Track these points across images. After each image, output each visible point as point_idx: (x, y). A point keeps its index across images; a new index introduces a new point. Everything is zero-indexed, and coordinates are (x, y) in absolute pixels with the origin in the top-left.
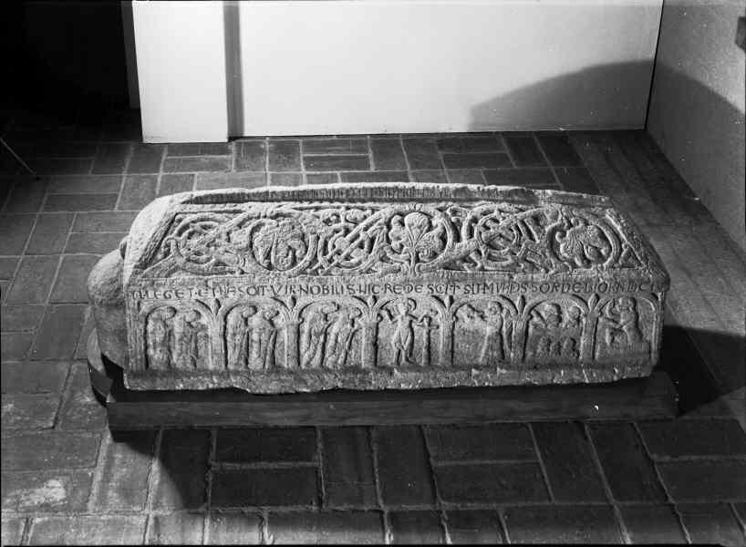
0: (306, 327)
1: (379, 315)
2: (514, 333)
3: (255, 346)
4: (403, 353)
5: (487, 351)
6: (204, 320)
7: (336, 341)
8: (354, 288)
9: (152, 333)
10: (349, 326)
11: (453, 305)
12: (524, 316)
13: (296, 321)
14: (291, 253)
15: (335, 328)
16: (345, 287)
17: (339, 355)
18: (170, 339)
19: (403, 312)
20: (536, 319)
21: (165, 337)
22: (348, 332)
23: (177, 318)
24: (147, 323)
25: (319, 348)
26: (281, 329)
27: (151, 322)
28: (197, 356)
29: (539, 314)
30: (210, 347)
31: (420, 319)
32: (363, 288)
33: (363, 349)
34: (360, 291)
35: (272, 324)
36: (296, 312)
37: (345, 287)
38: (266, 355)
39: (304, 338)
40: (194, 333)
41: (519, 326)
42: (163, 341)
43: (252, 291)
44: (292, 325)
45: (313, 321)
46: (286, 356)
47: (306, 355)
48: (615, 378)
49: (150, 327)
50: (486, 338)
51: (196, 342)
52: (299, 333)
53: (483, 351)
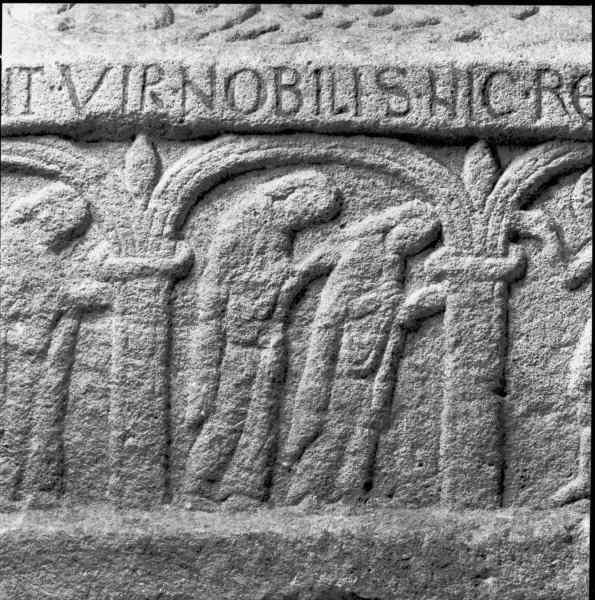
0: (204, 290)
1: (515, 236)
7: (329, 375)
8: (407, 82)
10: (386, 282)
15: (327, 300)
16: (367, 81)
17: (345, 437)
22: (379, 318)
32: (441, 91)
34: (433, 100)
36: (163, 207)
37: (367, 81)
38: (26, 433)
39: (195, 338)
47: (203, 438)
52: (171, 318)
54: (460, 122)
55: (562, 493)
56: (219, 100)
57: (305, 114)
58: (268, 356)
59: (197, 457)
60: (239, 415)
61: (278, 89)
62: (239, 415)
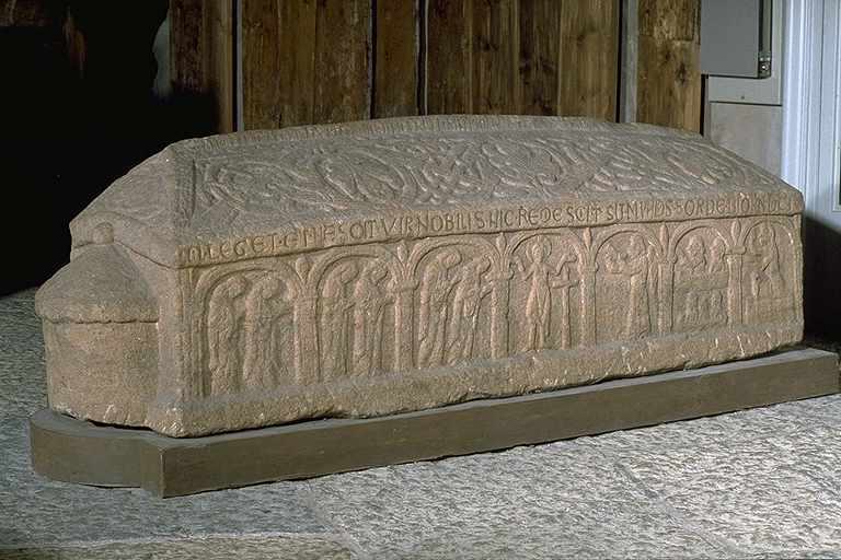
0: (423, 294)
2: (660, 286)
3: (358, 333)
4: (541, 329)
5: (634, 316)
6: (289, 297)
9: (214, 325)
11: (594, 244)
12: (670, 259)
13: (411, 284)
14: (385, 187)
16: (472, 216)
17: (466, 338)
18: (238, 338)
19: (538, 260)
20: (682, 261)
21: (232, 333)
23: (250, 297)
24: (206, 308)
25: (440, 328)
26: (391, 303)
27: (211, 304)
28: (279, 365)
29: (685, 254)
30: (296, 342)
31: (558, 268)
33: (493, 326)
35: (381, 293)
37: (472, 216)
38: (373, 348)
40: (275, 319)
41: (663, 271)
42: (230, 339)
43: (358, 232)
44: (406, 290)
45: (433, 280)
46: (397, 349)
47: (423, 344)
48: (770, 348)
49: (211, 320)
50: (632, 297)
51: (278, 336)
52: (414, 305)
53: (629, 319)
54: (498, 229)
55: (524, 350)
56: (429, 228)
57: (455, 231)
58: (443, 313)
59: (421, 355)
60: (435, 336)
61: (447, 221)
62: (435, 336)
